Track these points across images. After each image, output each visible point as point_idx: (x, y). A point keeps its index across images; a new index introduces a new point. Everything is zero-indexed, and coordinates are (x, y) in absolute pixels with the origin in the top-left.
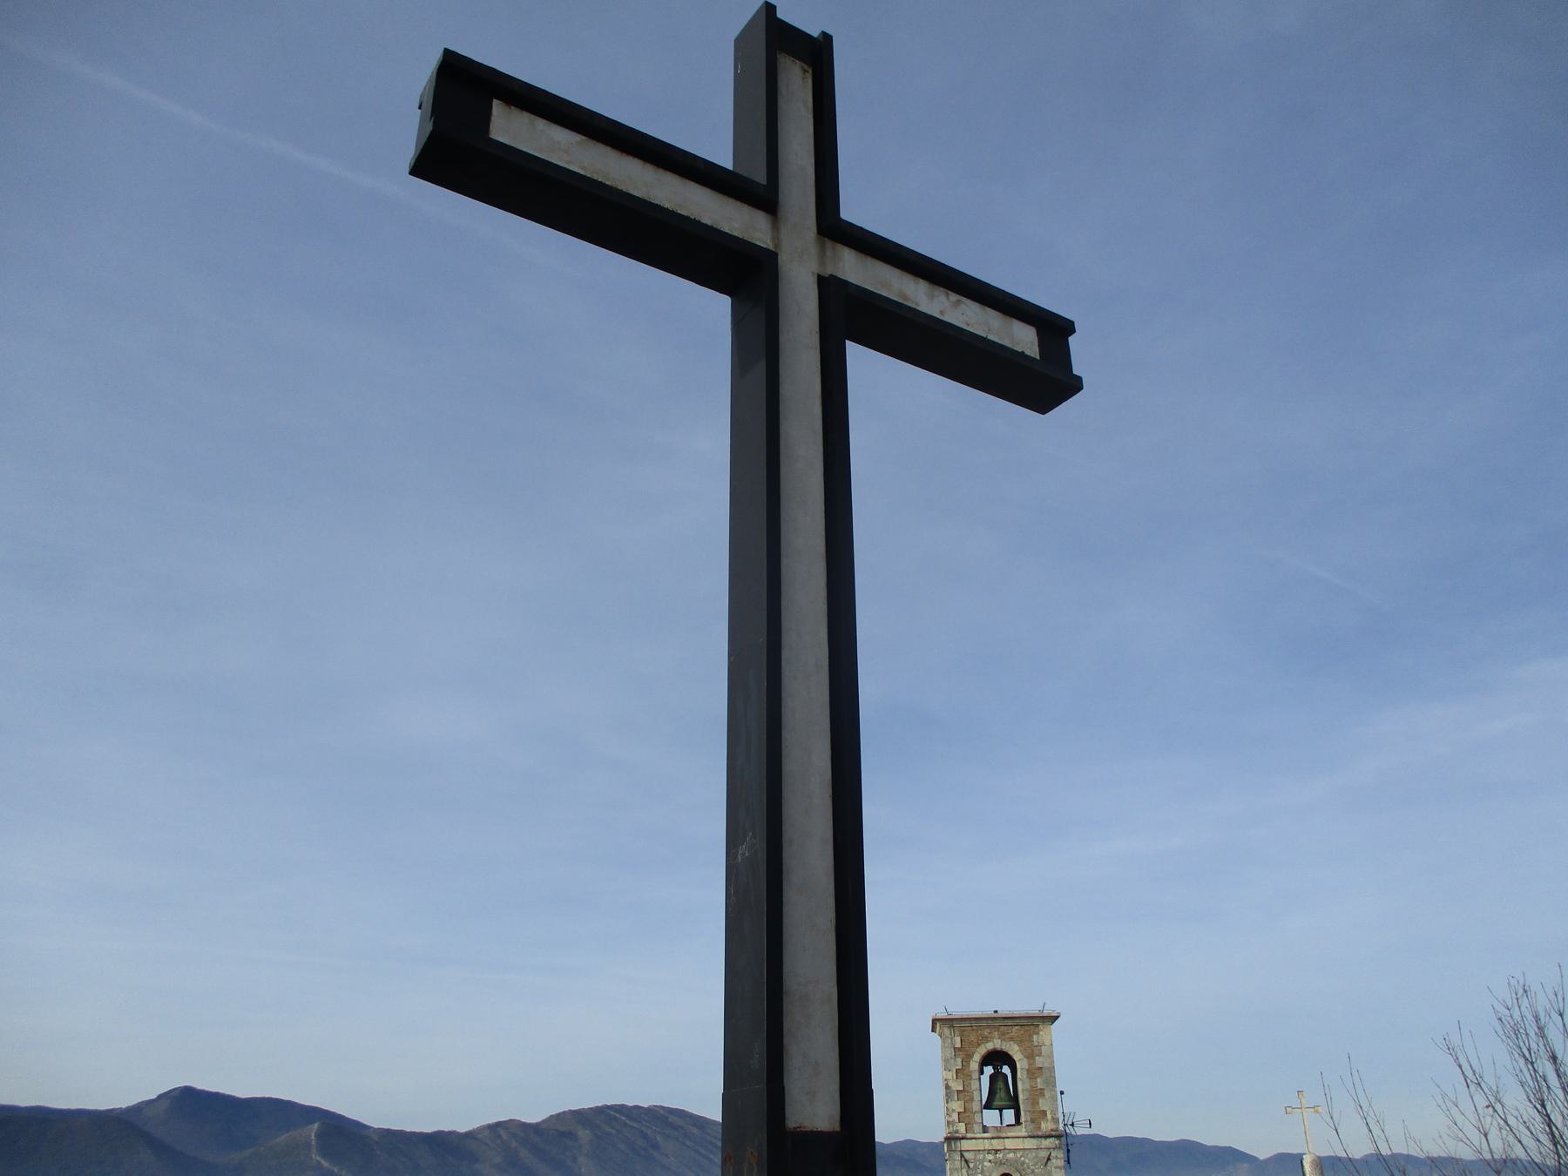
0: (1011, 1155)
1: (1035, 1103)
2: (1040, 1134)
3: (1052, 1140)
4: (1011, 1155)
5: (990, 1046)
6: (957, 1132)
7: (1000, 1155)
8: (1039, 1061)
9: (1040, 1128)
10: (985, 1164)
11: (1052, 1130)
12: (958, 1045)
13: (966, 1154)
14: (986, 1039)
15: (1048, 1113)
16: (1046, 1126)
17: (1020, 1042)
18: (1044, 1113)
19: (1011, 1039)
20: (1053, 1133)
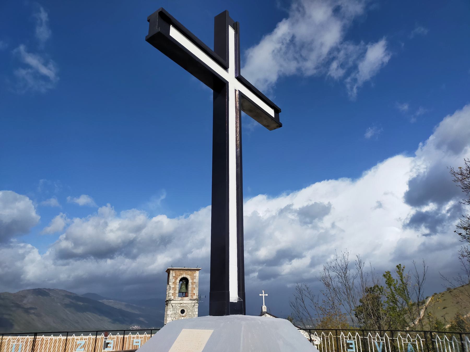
0: (185, 305)
1: (192, 291)
2: (193, 299)
3: (196, 301)
4: (185, 305)
5: (182, 276)
7: (182, 305)
8: (195, 280)
9: (193, 298)
10: (178, 307)
11: (196, 298)
13: (173, 304)
14: (181, 274)
15: (195, 294)
18: (194, 294)
20: (196, 299)
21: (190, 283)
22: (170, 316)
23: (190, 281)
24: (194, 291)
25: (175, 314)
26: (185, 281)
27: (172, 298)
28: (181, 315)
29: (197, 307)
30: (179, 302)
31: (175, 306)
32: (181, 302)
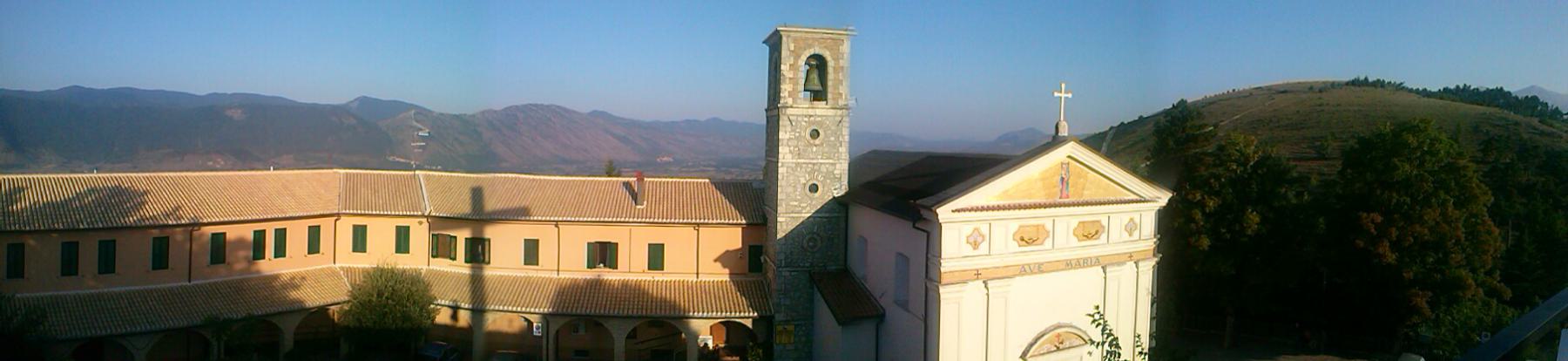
0: (820, 119)
1: (836, 87)
4: (820, 119)
6: (786, 103)
7: (812, 119)
12: (792, 48)
13: (791, 117)
14: (810, 46)
16: (841, 103)
17: (831, 50)
18: (841, 94)
19: (825, 47)
21: (830, 70)
22: (785, 142)
23: (831, 64)
24: (840, 87)
25: (797, 138)
26: (818, 64)
27: (790, 101)
28: (812, 141)
29: (847, 125)
30: (805, 112)
31: (797, 121)
32: (811, 112)
